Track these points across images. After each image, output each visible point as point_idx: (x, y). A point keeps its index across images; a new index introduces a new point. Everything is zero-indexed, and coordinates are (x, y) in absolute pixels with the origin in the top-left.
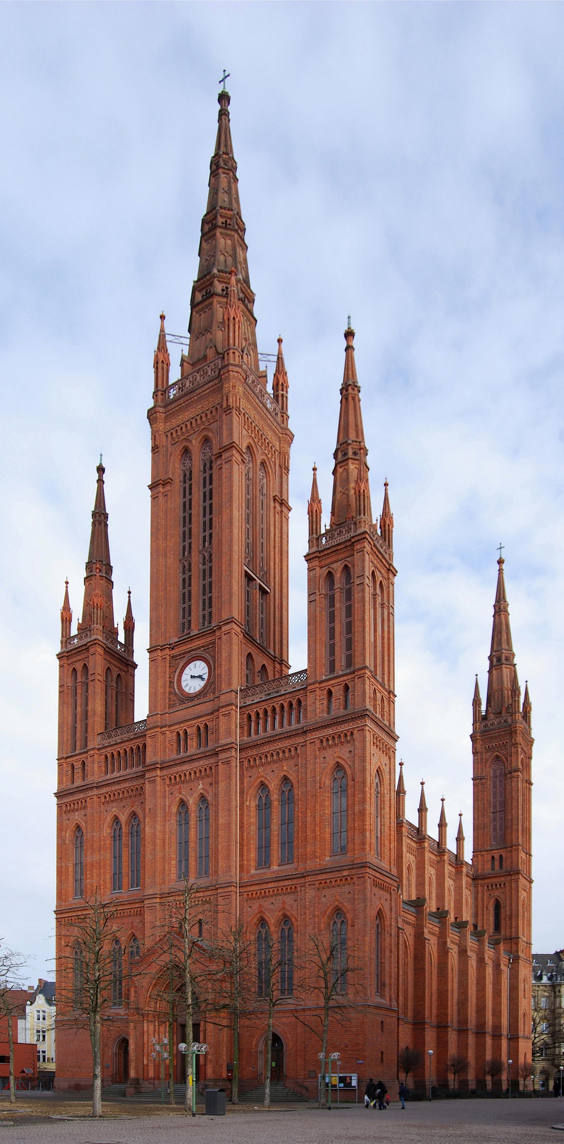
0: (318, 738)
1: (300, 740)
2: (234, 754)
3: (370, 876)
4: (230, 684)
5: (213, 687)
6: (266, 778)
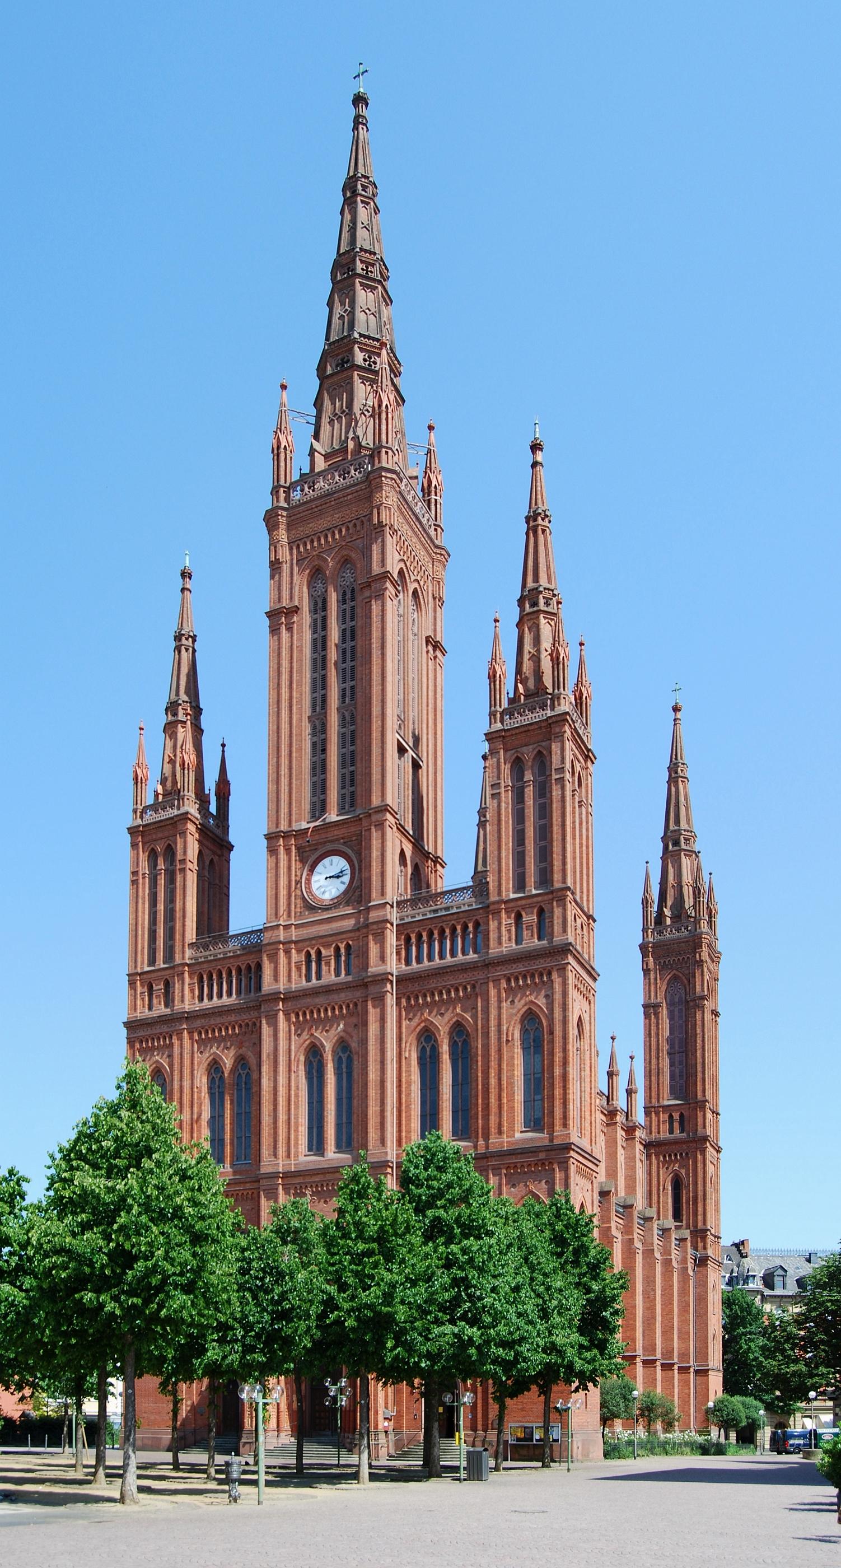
0: (505, 975)
1: (480, 975)
2: (389, 986)
3: (575, 1162)
4: (383, 894)
5: (357, 894)
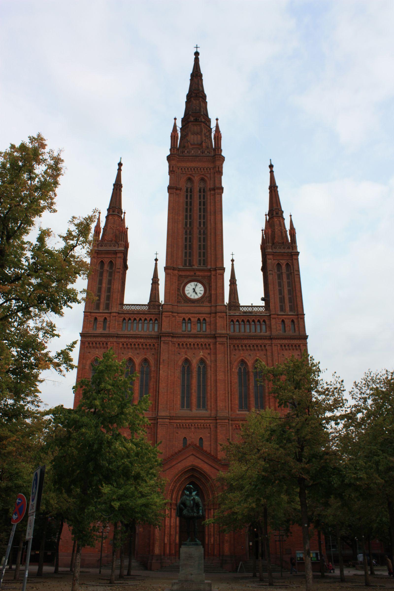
6: (245, 358)
